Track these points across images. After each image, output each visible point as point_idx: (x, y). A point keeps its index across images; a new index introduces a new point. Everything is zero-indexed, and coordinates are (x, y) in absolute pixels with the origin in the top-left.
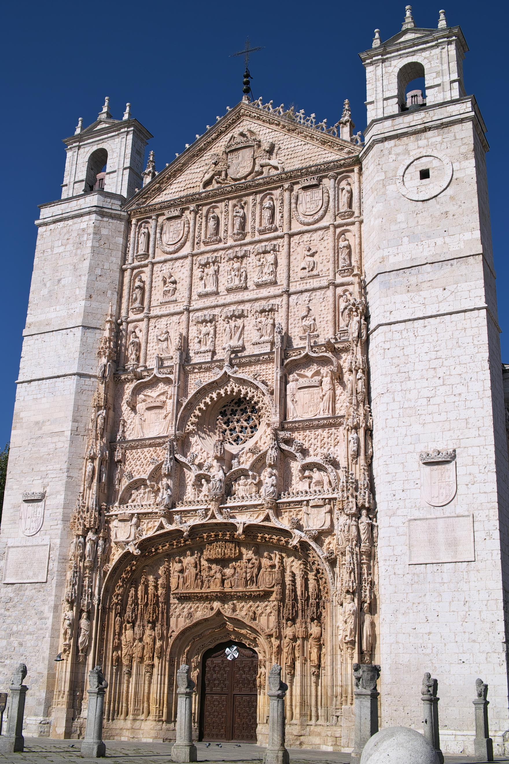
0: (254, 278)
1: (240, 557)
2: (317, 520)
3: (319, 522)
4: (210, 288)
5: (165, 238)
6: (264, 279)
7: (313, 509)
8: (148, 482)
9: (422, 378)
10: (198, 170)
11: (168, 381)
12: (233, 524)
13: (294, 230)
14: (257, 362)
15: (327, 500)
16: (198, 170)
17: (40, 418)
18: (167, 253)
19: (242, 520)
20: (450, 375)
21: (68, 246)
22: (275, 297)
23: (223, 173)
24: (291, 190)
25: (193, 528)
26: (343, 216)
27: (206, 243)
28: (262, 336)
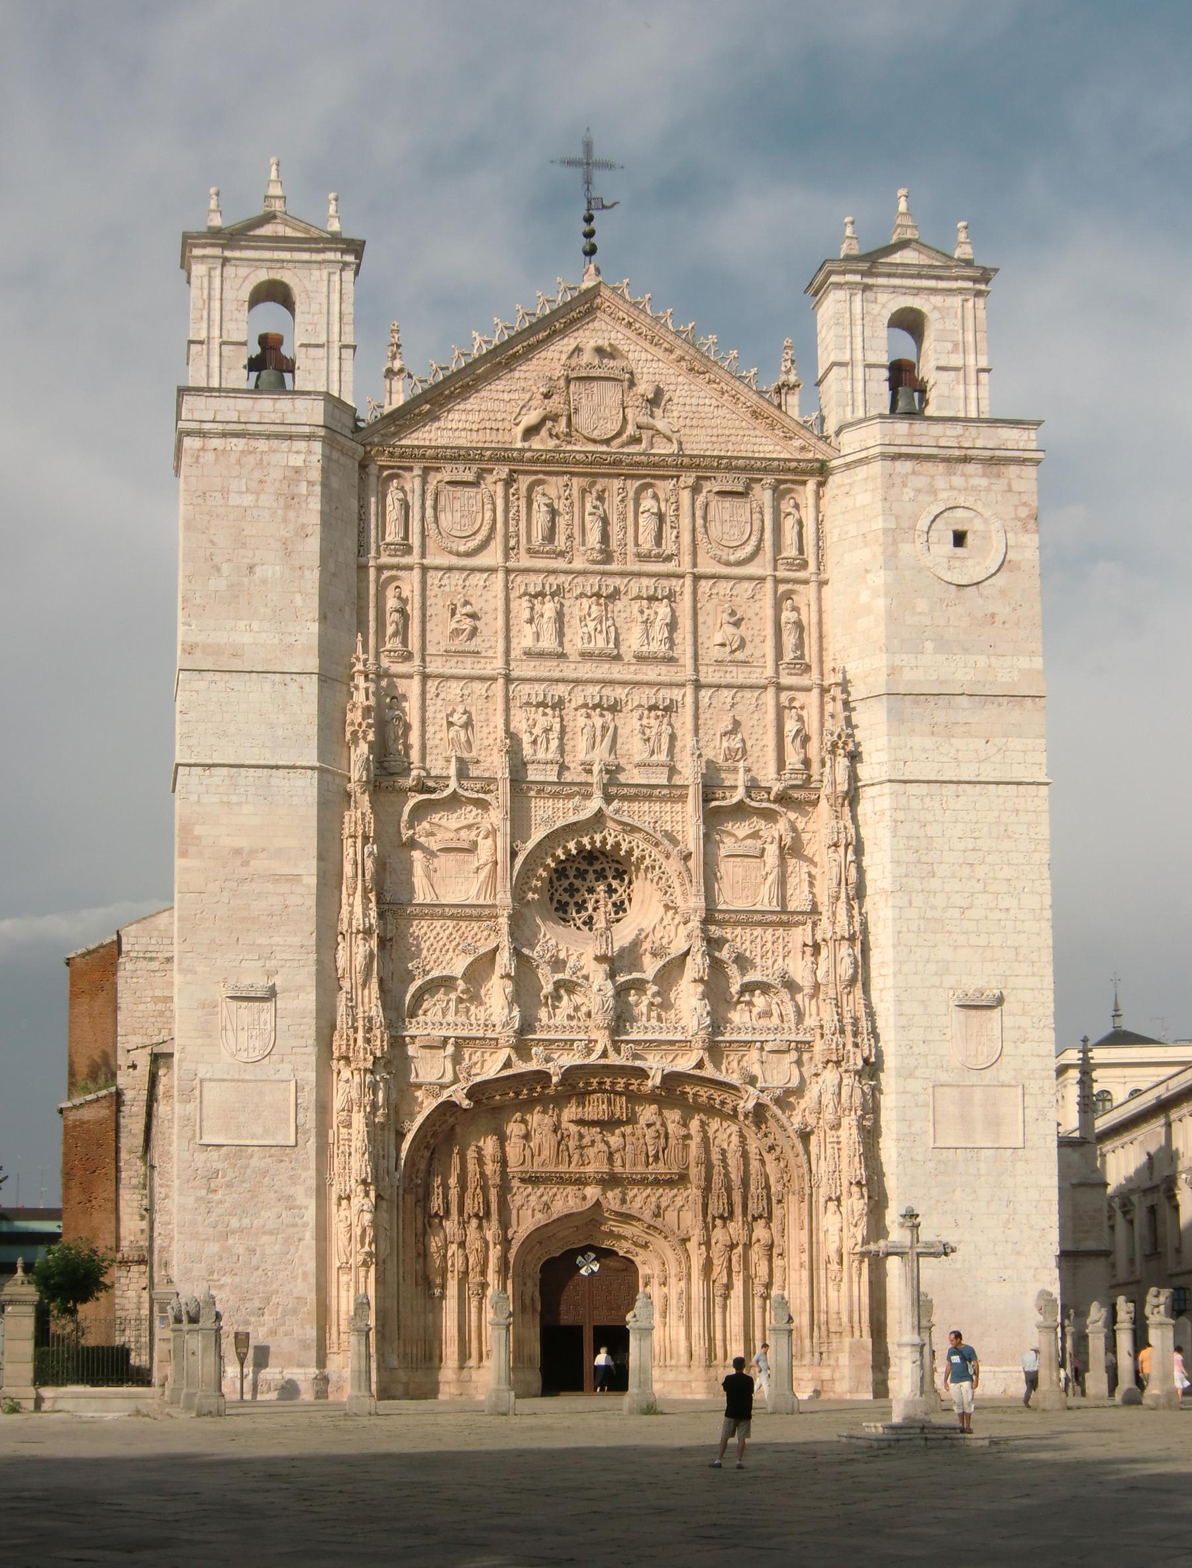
0: (633, 641)
1: (632, 1120)
3: (781, 1076)
4: (548, 643)
5: (445, 519)
6: (652, 649)
7: (771, 1055)
8: (460, 982)
9: (954, 876)
10: (506, 396)
11: (482, 805)
12: (642, 1070)
13: (700, 570)
14: (649, 798)
15: (793, 1045)
16: (506, 396)
17: (244, 843)
18: (451, 553)
19: (656, 1065)
20: (995, 879)
22: (671, 685)
23: (564, 421)
24: (695, 490)
25: (571, 1073)
26: (791, 565)
27: (531, 552)
28: (653, 753)
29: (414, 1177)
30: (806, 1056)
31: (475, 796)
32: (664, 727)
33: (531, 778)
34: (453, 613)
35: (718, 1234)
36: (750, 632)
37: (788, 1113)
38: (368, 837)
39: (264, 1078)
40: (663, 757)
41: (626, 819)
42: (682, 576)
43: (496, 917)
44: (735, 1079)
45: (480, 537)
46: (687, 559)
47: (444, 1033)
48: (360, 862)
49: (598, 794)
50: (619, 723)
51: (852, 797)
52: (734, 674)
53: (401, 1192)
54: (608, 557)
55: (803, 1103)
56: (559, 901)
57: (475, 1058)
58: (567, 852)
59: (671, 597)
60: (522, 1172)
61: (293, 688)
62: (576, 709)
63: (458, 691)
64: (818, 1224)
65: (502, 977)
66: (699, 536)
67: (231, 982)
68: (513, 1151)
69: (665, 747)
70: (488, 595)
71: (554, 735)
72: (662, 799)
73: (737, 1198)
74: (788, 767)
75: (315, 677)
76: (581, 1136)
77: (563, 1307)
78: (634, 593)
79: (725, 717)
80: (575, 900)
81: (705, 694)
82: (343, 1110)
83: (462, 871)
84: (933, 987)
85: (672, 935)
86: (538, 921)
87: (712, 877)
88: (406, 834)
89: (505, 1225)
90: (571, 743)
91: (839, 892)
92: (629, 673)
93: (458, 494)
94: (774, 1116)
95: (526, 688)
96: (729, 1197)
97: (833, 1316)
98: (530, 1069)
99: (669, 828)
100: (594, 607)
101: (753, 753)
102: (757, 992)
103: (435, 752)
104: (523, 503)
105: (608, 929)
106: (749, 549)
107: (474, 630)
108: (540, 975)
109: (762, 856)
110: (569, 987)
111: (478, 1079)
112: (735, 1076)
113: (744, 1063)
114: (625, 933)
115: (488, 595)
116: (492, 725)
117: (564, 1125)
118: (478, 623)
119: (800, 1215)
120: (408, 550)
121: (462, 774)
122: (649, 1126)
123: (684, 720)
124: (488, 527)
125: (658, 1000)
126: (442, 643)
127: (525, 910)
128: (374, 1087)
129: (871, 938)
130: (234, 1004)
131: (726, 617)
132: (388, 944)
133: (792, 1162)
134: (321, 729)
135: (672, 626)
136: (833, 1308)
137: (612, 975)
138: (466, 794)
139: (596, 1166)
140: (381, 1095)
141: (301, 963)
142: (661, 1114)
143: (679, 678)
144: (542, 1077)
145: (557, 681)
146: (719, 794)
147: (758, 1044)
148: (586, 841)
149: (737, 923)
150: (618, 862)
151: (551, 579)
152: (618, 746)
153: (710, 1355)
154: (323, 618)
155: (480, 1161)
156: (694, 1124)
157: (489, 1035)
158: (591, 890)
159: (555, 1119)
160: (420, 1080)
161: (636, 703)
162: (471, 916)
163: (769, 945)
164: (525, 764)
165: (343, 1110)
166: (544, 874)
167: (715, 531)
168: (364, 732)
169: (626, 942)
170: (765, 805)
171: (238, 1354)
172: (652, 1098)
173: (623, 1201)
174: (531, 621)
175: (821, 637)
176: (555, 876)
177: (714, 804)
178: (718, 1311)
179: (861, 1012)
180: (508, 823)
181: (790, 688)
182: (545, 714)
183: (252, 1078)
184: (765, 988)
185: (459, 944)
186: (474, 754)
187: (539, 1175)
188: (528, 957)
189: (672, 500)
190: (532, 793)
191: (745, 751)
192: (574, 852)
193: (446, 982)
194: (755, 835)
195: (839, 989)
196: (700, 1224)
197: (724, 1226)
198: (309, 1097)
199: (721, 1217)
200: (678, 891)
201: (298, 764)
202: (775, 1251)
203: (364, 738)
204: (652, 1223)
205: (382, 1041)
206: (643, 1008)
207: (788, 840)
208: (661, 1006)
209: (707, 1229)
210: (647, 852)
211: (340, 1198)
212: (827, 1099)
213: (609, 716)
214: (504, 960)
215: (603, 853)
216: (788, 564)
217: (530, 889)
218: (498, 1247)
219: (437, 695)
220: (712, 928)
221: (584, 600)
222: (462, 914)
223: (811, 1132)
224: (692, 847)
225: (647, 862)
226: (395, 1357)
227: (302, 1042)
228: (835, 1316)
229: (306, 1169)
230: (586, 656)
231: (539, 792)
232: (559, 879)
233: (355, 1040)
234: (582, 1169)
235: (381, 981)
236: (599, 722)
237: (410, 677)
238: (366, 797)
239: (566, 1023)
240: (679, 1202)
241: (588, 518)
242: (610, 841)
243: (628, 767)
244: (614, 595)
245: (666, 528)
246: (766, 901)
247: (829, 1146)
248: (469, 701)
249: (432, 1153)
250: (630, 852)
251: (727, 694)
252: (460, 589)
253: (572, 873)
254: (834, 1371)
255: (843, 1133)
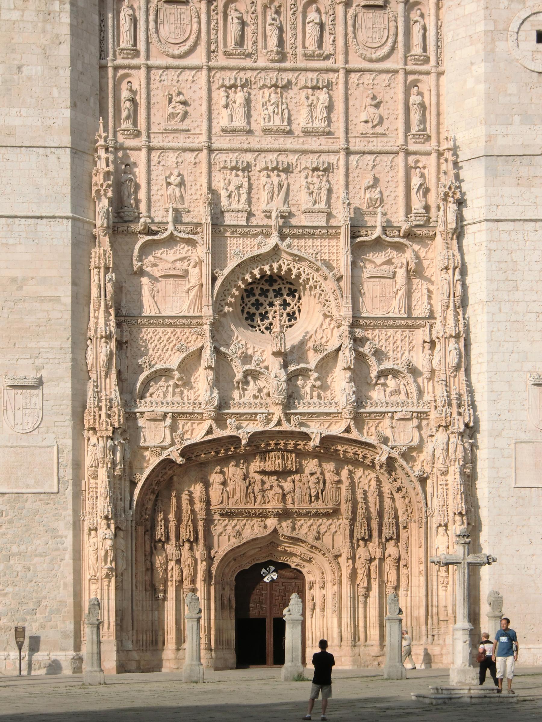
0: (301, 120)
1: (299, 470)
2: (404, 435)
4: (239, 122)
5: (164, 30)
6: (315, 125)
7: (399, 422)
8: (176, 373)
12: (306, 434)
13: (351, 66)
14: (312, 236)
15: (415, 414)
18: (168, 55)
19: (316, 430)
21: (26, 13)
22: (329, 152)
25: (255, 437)
28: (315, 202)
29: (143, 514)
30: (424, 423)
31: (187, 236)
32: (323, 183)
33: (227, 223)
34: (170, 101)
35: (361, 552)
36: (387, 112)
37: (411, 464)
38: (109, 268)
39: (35, 444)
40: (322, 206)
41: (295, 252)
42: (337, 71)
43: (202, 325)
44: (372, 440)
45: (189, 43)
46: (341, 57)
47: (165, 409)
48: (102, 286)
49: (275, 233)
50: (291, 181)
51: (459, 233)
52: (375, 144)
53: (134, 525)
54: (283, 57)
55: (422, 457)
56: (248, 313)
57: (186, 428)
58: (253, 276)
59: (329, 86)
60: (221, 509)
61: (53, 158)
62: (260, 172)
63: (174, 159)
64: (431, 543)
65: (206, 369)
66: (350, 40)
67: (10, 375)
68: (215, 494)
69: (324, 198)
70: (195, 87)
71: (244, 191)
72: (322, 237)
73: (375, 525)
74: (414, 211)
75: (68, 151)
76: (263, 483)
77: (251, 605)
78: (302, 84)
79: (368, 176)
80: (260, 311)
81: (353, 158)
82: (92, 466)
83: (177, 291)
84: (516, 371)
85: (329, 336)
86: (233, 327)
87: (359, 295)
88: (137, 265)
89: (209, 547)
90: (256, 196)
91: (449, 303)
92: (298, 144)
93: (173, 11)
94: (401, 466)
95: (223, 157)
96: (369, 525)
97: (442, 609)
98: (226, 434)
99: (327, 258)
100: (273, 95)
101: (389, 201)
102: (390, 377)
103: (158, 205)
104: (221, 16)
105: (282, 332)
106: (386, 49)
107: (185, 115)
108: (234, 367)
109: (394, 277)
110: (254, 374)
111: (188, 443)
112: (373, 437)
113: (380, 429)
114: (295, 335)
115: (195, 87)
116: (199, 184)
117: (252, 474)
118: (188, 109)
119: (419, 537)
120: (136, 54)
121: (177, 221)
122: (312, 474)
123: (338, 178)
124: (195, 35)
125: (318, 383)
126: (162, 124)
127: (223, 320)
128: (113, 450)
129: (472, 336)
130: (12, 391)
131: (369, 101)
132: (124, 346)
133: (414, 500)
134: (73, 188)
135: (330, 108)
136: (442, 603)
137: (285, 366)
138: (180, 235)
139: (274, 504)
140: (118, 455)
141: (61, 360)
142: (320, 465)
143: (335, 147)
144: (235, 440)
145: (246, 151)
146: (363, 232)
147: (390, 414)
148: (266, 268)
149: (376, 327)
150: (291, 283)
151: (242, 74)
152: (290, 198)
153: (355, 638)
154: (74, 106)
155: (191, 501)
156: (344, 473)
157: (197, 410)
158: (271, 304)
159: (244, 470)
160: (148, 444)
161: (303, 167)
162: (184, 324)
163: (399, 342)
164: (223, 213)
165: (92, 466)
166: (237, 293)
167: (362, 35)
168: (105, 190)
169: (296, 342)
170: (396, 240)
171: (17, 642)
172: (314, 454)
173: (294, 529)
174: (226, 106)
175: (438, 114)
176: (245, 294)
177: (359, 239)
178: (361, 606)
179: (464, 390)
180: (210, 255)
181: (415, 153)
182: (237, 176)
183: (27, 444)
184: (395, 373)
185: (175, 345)
186: (186, 205)
187: (233, 510)
188: (224, 353)
189: (331, 12)
190: (228, 234)
191: (382, 200)
192: (258, 276)
193: (166, 373)
194: (389, 262)
195: (448, 373)
196: (348, 545)
197: (366, 545)
198: (67, 458)
199: (363, 539)
200: (333, 304)
201: (56, 215)
202: (402, 563)
203: (105, 195)
204: (314, 544)
205: (119, 416)
206: (308, 389)
207: (412, 266)
208: (320, 387)
209: (353, 548)
210: (311, 276)
211: (90, 530)
212: (439, 453)
213: (283, 176)
214: (207, 355)
215: (280, 277)
216: (415, 59)
217: (227, 304)
218: (204, 563)
219: (159, 163)
220: (357, 330)
221: (266, 90)
222: (176, 323)
223: (427, 478)
224: (343, 272)
225: (311, 283)
226: (130, 642)
227: (62, 418)
228: (443, 609)
229: (66, 509)
230: (267, 131)
231: (233, 233)
232: (248, 297)
233: (100, 416)
234: (264, 506)
235: (119, 373)
236: (276, 180)
237: (139, 149)
238: (107, 238)
239: (252, 401)
240: (333, 529)
241: (268, 28)
242: (284, 268)
243: (297, 214)
244: (287, 86)
245: (326, 34)
246: (397, 310)
247: (440, 487)
248: (182, 166)
249: (157, 497)
250: (298, 276)
251: (369, 158)
252: (175, 83)
253: (257, 292)
254: (442, 649)
255: (450, 477)
